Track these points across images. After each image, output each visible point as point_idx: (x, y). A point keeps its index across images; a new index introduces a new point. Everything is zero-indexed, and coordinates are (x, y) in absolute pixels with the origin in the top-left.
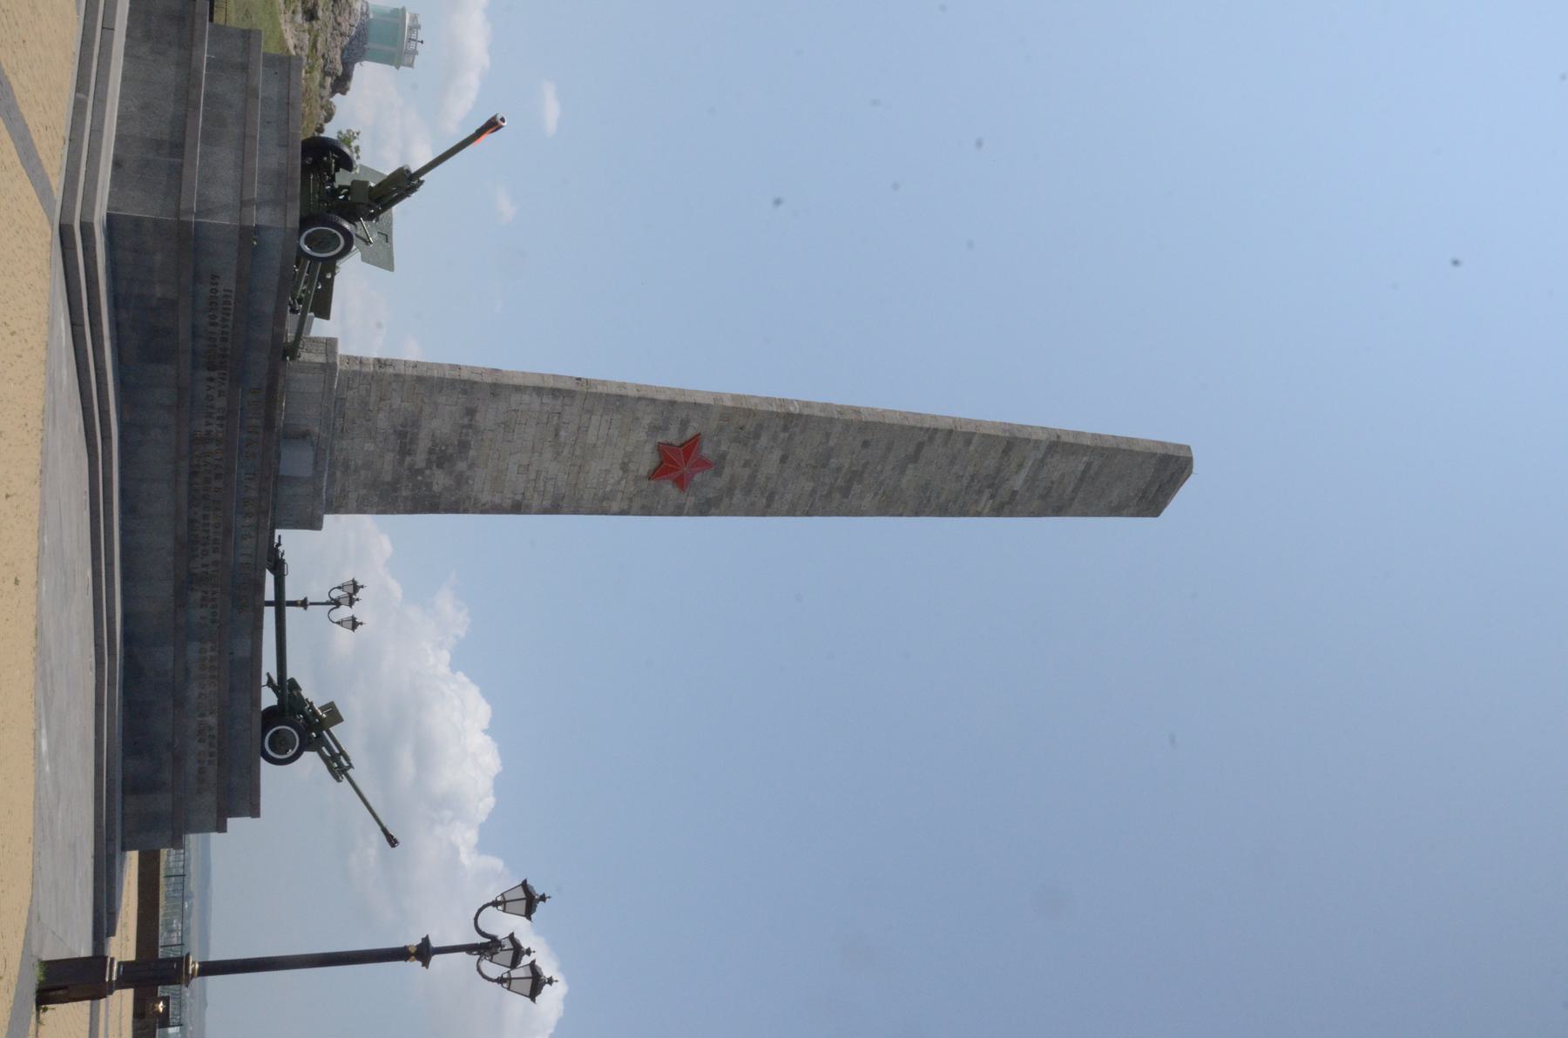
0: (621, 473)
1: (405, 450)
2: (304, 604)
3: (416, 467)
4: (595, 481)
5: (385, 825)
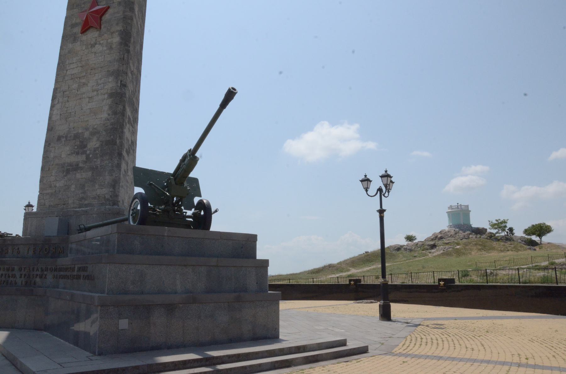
0: (97, 46)
1: (75, 168)
3: (85, 160)
4: (100, 58)
5: (218, 107)
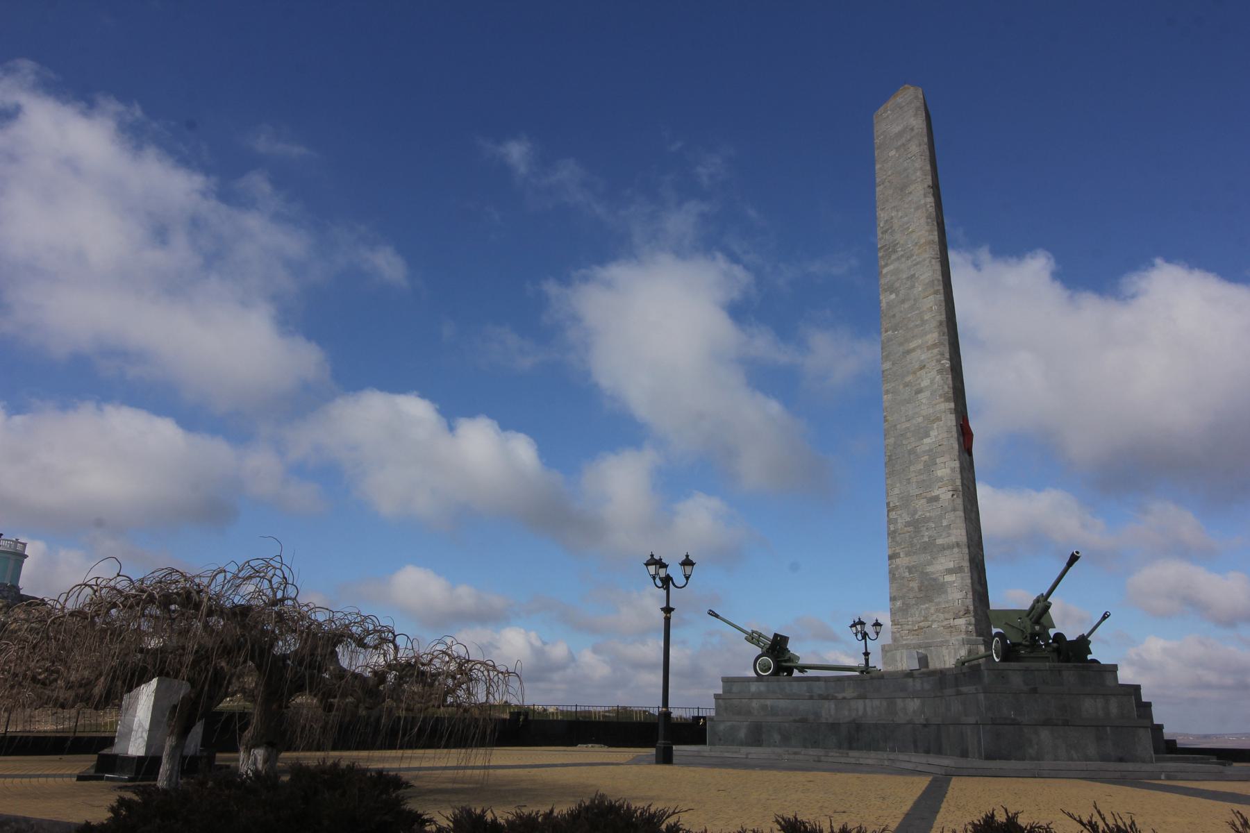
2: (866, 654)
